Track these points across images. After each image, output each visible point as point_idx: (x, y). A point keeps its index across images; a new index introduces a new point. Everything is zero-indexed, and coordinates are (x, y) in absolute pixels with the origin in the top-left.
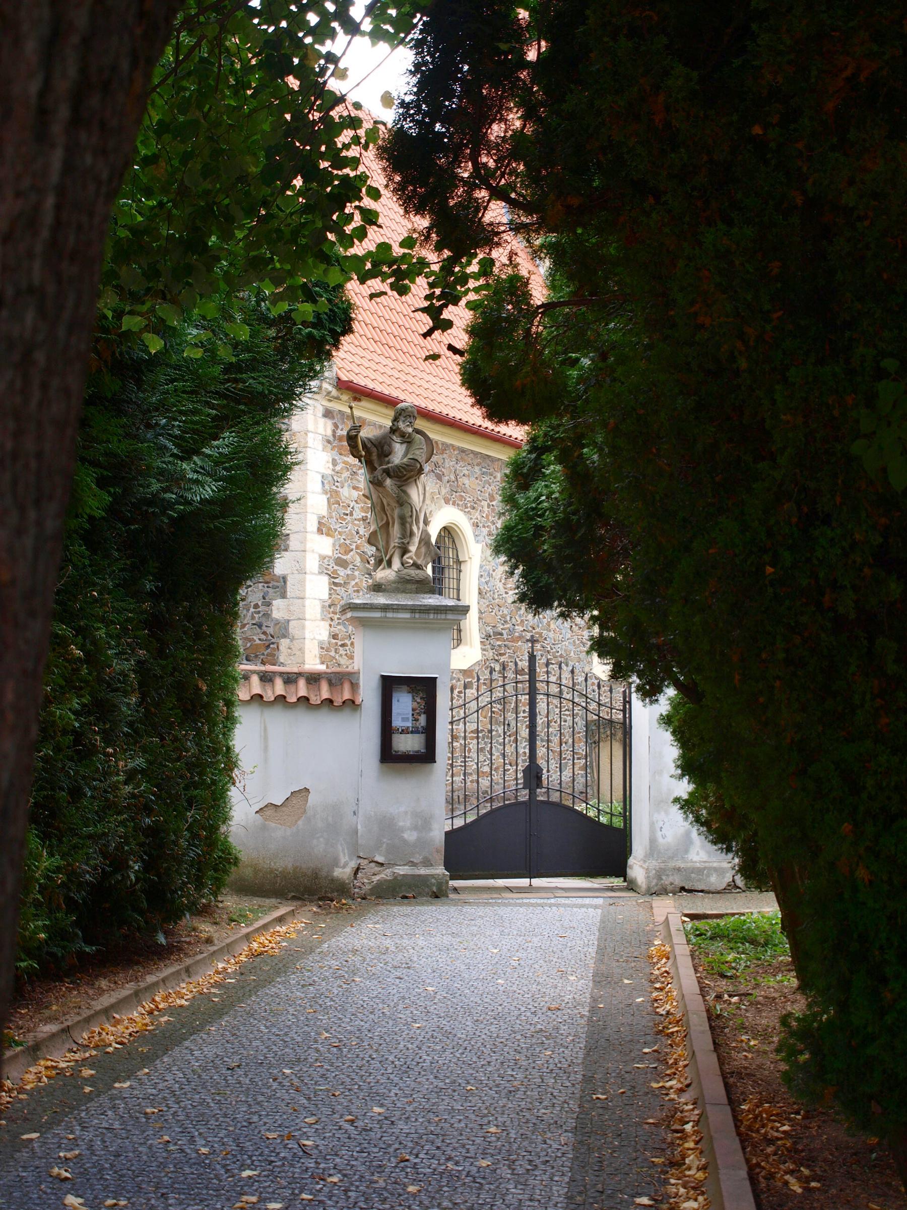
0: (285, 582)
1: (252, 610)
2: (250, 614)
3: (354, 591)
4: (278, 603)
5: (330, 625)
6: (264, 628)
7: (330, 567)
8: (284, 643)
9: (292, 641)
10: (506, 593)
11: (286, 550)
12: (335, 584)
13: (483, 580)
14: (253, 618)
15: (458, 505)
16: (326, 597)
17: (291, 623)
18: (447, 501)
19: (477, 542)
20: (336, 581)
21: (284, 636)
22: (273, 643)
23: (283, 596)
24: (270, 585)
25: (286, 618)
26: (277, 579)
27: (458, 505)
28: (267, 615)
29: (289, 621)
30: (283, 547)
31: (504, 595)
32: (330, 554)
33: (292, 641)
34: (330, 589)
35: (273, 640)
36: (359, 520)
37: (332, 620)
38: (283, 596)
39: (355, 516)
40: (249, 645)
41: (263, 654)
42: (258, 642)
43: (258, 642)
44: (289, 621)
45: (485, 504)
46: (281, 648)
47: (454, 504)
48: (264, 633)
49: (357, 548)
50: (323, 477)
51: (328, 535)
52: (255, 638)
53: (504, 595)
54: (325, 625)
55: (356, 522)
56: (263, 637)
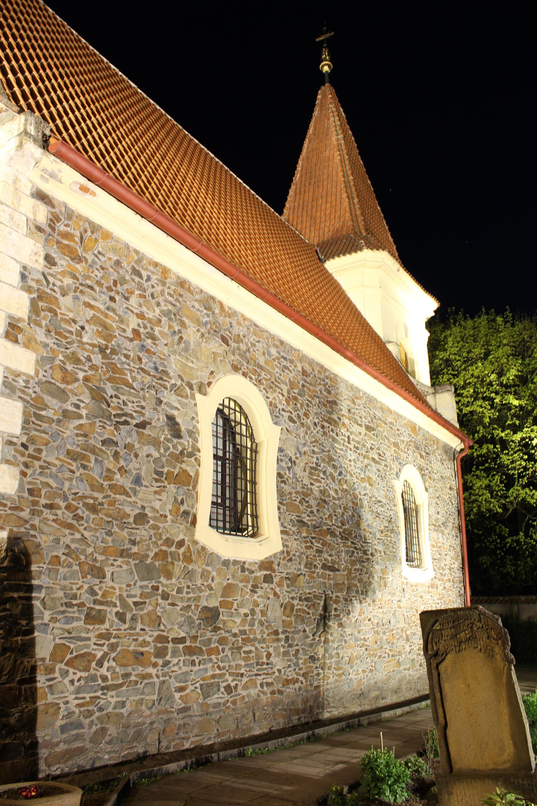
3: (77, 435)
5: (24, 474)
7: (31, 391)
10: (311, 484)
12: (38, 417)
13: (284, 464)
15: (251, 378)
16: (17, 430)
18: (236, 368)
19: (276, 423)
20: (43, 413)
27: (251, 378)
31: (309, 486)
32: (32, 373)
34: (26, 422)
36: (93, 345)
37: (26, 465)
39: (85, 340)
45: (285, 388)
47: (245, 375)
49: (86, 379)
50: (25, 268)
51: (27, 346)
53: (309, 486)
54: (16, 471)
55: (88, 347)
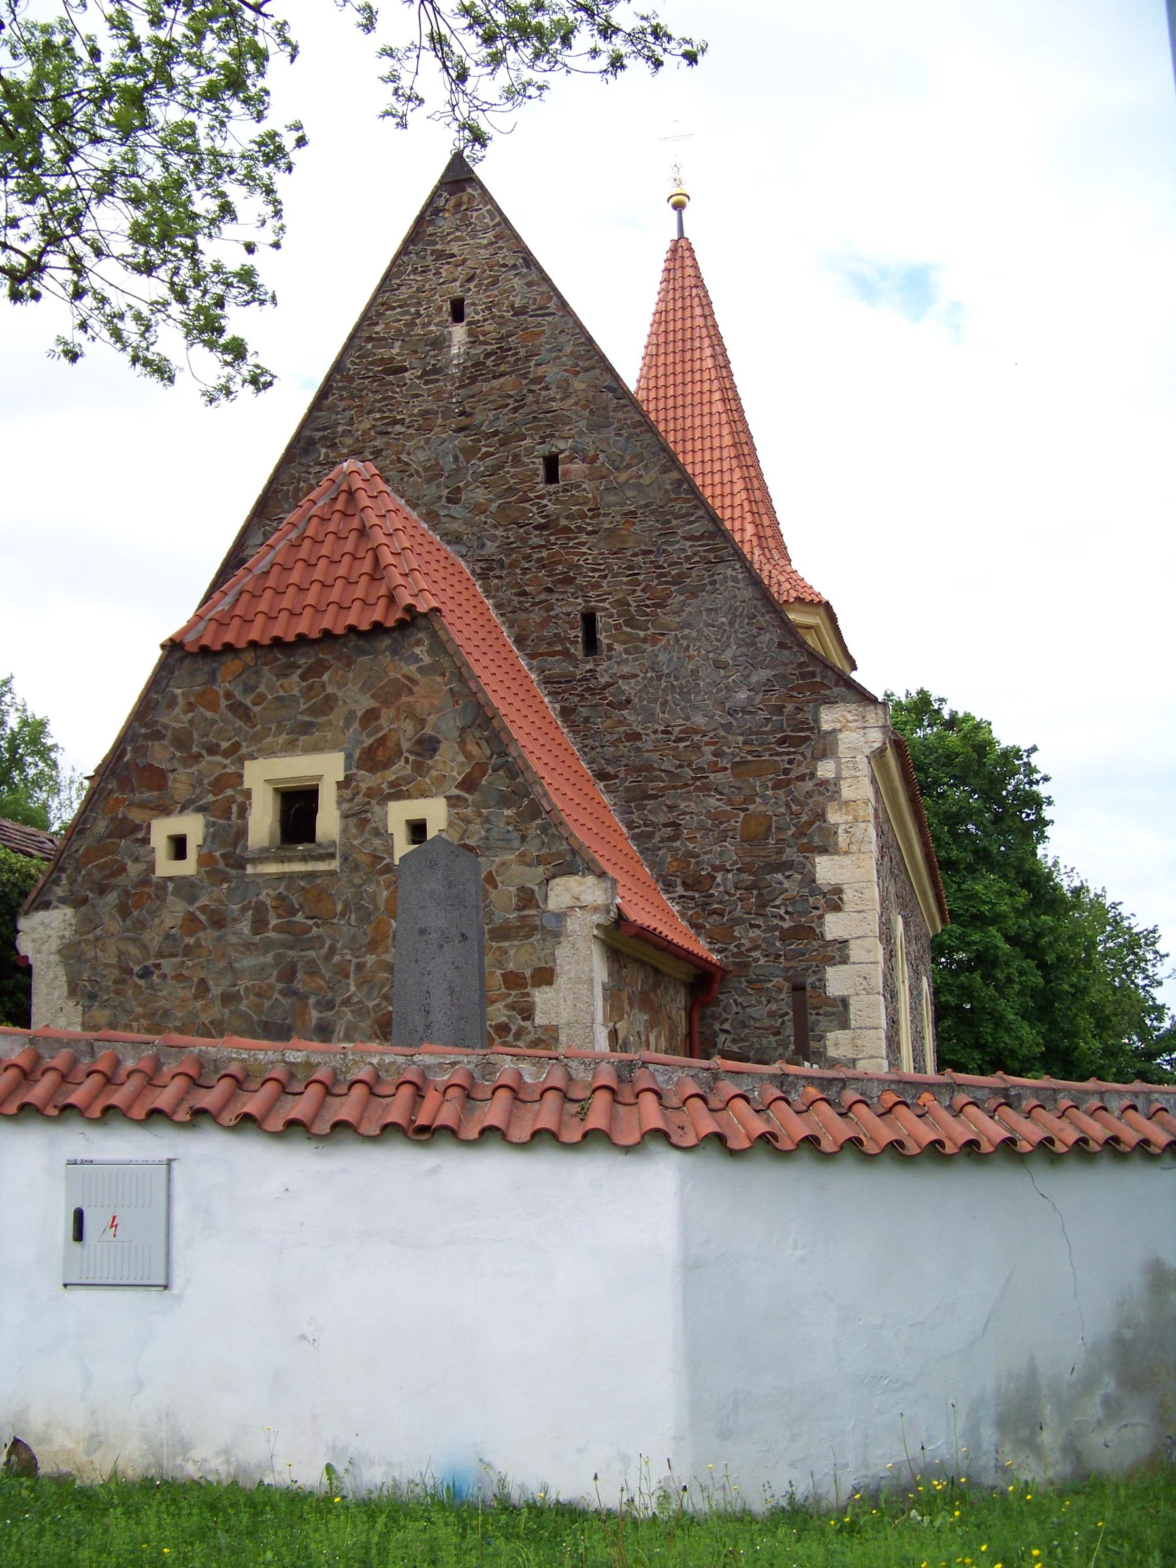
23: (845, 1025)
24: (821, 1011)
25: (850, 1056)
26: (832, 1002)
30: (838, 959)
38: (845, 1025)
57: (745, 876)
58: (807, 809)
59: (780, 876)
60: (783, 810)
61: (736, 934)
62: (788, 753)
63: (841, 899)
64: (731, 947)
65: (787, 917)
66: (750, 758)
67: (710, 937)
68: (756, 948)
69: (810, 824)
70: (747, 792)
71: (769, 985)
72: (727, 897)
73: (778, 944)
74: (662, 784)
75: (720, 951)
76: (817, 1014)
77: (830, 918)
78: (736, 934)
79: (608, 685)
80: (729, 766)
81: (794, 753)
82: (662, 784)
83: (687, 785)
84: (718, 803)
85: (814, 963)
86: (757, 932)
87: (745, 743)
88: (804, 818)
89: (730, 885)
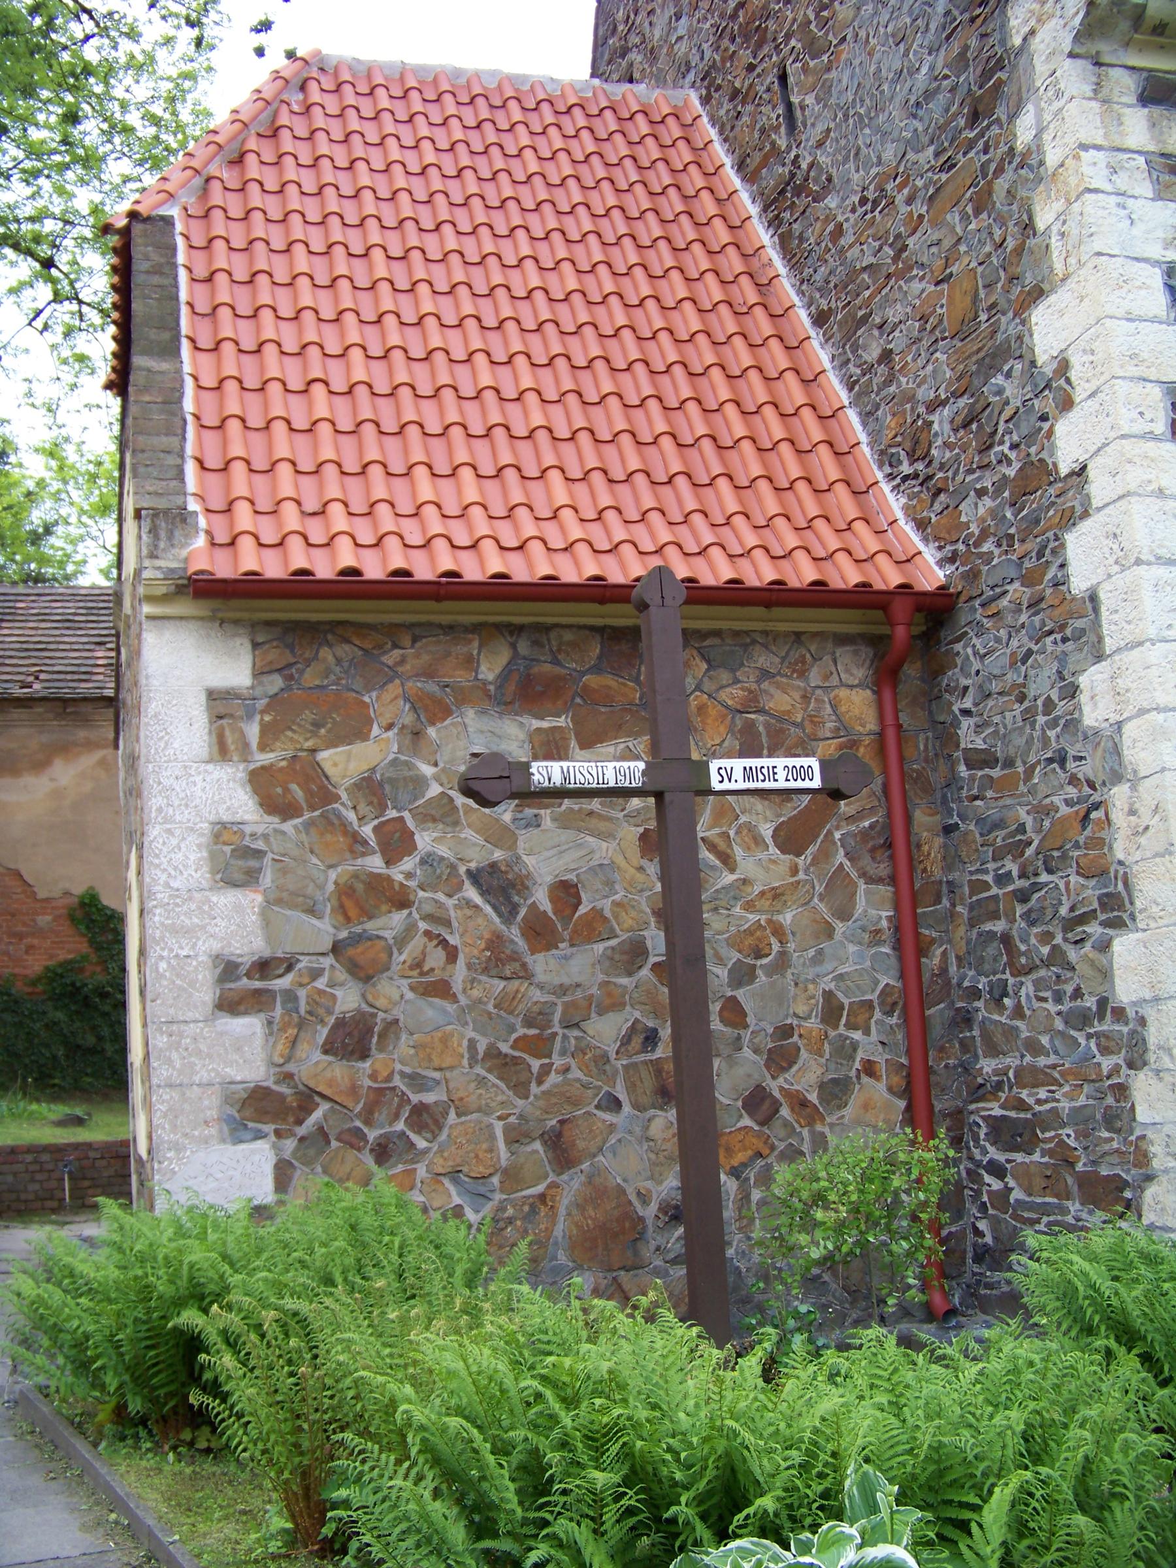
0: (1096, 610)
1: (1041, 719)
2: (1037, 734)
4: (1092, 679)
6: (1071, 765)
8: (1119, 795)
9: (1134, 788)
11: (1086, 514)
14: (1046, 741)
17: (1129, 730)
21: (1117, 777)
22: (1096, 806)
25: (1114, 718)
28: (1072, 724)
29: (1119, 725)
30: (1079, 510)
33: (1134, 788)
35: (1096, 797)
40: (1047, 824)
41: (1077, 846)
42: (1064, 810)
43: (1064, 810)
44: (1119, 725)
46: (1113, 816)
48: (1073, 780)
52: (1055, 799)
56: (1072, 792)
57: (963, 402)
58: (1011, 224)
59: (999, 380)
60: (988, 248)
61: (963, 519)
62: (981, 135)
63: (1068, 381)
64: (961, 547)
65: (1012, 455)
66: (944, 177)
67: (937, 539)
68: (984, 534)
69: (1019, 251)
70: (947, 244)
71: (1004, 602)
72: (948, 455)
73: (1009, 515)
74: (867, 293)
75: (952, 559)
76: (1065, 640)
77: (1062, 428)
78: (963, 519)
79: (811, 166)
80: (923, 210)
81: (988, 127)
82: (867, 293)
83: (889, 276)
84: (923, 284)
85: (1050, 534)
86: (988, 502)
87: (937, 155)
88: (1011, 244)
89: (947, 427)
